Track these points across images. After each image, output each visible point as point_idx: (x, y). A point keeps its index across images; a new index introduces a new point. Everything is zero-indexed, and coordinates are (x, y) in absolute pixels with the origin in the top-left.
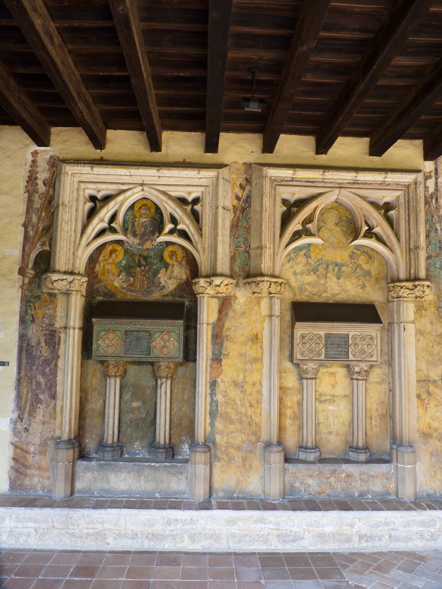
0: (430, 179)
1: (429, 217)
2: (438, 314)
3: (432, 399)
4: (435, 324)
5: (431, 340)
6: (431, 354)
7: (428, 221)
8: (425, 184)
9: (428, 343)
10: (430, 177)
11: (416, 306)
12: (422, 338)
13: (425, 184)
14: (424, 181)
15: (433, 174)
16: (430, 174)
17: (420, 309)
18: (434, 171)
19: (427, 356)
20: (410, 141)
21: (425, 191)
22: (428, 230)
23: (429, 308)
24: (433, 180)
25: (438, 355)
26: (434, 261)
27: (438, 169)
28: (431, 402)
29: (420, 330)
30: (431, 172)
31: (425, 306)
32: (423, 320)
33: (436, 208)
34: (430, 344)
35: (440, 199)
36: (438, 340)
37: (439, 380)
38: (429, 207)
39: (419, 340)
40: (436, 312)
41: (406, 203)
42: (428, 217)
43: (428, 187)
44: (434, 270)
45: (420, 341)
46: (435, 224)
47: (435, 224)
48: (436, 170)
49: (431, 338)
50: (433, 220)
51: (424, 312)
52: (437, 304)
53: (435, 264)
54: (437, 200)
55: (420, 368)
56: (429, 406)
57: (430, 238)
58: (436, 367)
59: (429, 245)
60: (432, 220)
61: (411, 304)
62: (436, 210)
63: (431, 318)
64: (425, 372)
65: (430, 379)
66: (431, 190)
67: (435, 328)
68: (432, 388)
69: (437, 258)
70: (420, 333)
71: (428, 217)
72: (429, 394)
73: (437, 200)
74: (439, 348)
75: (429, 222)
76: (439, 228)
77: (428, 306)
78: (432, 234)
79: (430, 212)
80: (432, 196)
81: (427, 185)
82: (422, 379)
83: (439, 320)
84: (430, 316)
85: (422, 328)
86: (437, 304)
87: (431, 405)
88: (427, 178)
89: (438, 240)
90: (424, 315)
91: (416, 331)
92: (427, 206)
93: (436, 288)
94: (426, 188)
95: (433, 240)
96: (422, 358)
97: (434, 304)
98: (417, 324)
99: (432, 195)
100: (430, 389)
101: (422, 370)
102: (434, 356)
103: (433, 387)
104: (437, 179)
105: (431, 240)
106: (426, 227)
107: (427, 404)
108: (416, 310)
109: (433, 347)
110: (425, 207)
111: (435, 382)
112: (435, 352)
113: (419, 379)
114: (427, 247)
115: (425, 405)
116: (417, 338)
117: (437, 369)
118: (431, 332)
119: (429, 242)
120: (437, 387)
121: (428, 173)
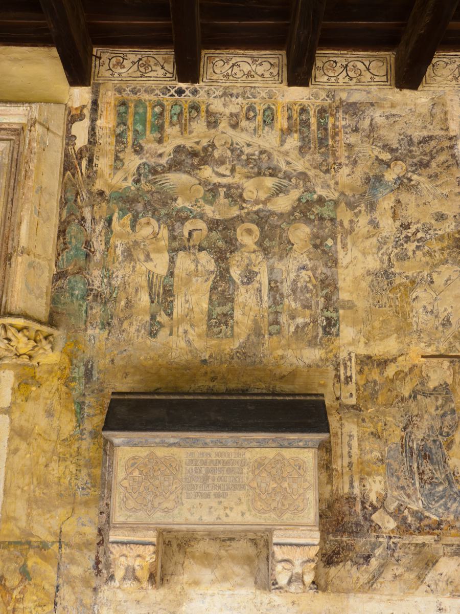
0: (81, 120)
1: (71, 196)
2: (66, 393)
3: (31, 589)
4: (57, 415)
5: (44, 451)
6: (43, 483)
7: (66, 203)
8: (68, 130)
9: (38, 457)
10: (81, 117)
11: (17, 377)
12: (23, 446)
13: (68, 130)
14: (67, 125)
15: (86, 112)
16: (81, 111)
17: (26, 384)
18: (89, 106)
19: (32, 487)
20: (46, 49)
21: (67, 144)
22: (64, 222)
23: (47, 380)
24: (86, 122)
25: (59, 484)
26: (70, 282)
27: (99, 102)
28: (28, 596)
29: (22, 428)
30: (84, 107)
31: (38, 375)
32: (30, 406)
33: (88, 177)
34: (42, 460)
35: (98, 159)
36: (60, 449)
37: (53, 543)
38: (73, 175)
39: (14, 452)
40: (64, 389)
41: (14, 165)
42: (68, 194)
43: (75, 136)
44: (69, 301)
45: (19, 453)
46: (80, 208)
47: (80, 208)
48: (95, 103)
49: (47, 446)
50: (79, 200)
51: (34, 388)
52: (67, 371)
53: (72, 289)
54: (90, 161)
55: (12, 515)
56: (21, 606)
57: (68, 236)
58: (50, 511)
59: (63, 250)
60: (76, 201)
61: (7, 371)
62: (87, 180)
63: (49, 402)
64: (23, 524)
65: (33, 539)
66: (81, 141)
67: (56, 423)
68: (33, 561)
69: (78, 277)
70: (20, 435)
71: (69, 195)
72: (25, 574)
73: (90, 161)
74: (62, 468)
75: (69, 204)
76: (88, 216)
77: (46, 376)
78: (73, 228)
79: (74, 185)
80: (80, 154)
81: (73, 133)
82: (12, 540)
83: (66, 407)
84: (47, 399)
85: (23, 423)
86: (67, 371)
87: (26, 604)
88: (73, 117)
89: (84, 239)
90: (33, 395)
91: (12, 430)
92: (68, 172)
93: (68, 338)
94: (70, 138)
95: (74, 240)
96: (19, 492)
97: (59, 372)
98: (16, 415)
99: (81, 150)
100: (30, 563)
101: (15, 519)
102: (47, 486)
103: (39, 560)
104: (93, 120)
105: (68, 239)
106: (60, 215)
107: (17, 601)
108: (16, 386)
109: (46, 466)
110: (64, 175)
111: (43, 546)
112: (51, 476)
113: (7, 539)
114: (59, 254)
115: (12, 604)
116: (12, 447)
117: (52, 517)
118: (45, 432)
119: (65, 244)
120: (45, 559)
121: (76, 109)
